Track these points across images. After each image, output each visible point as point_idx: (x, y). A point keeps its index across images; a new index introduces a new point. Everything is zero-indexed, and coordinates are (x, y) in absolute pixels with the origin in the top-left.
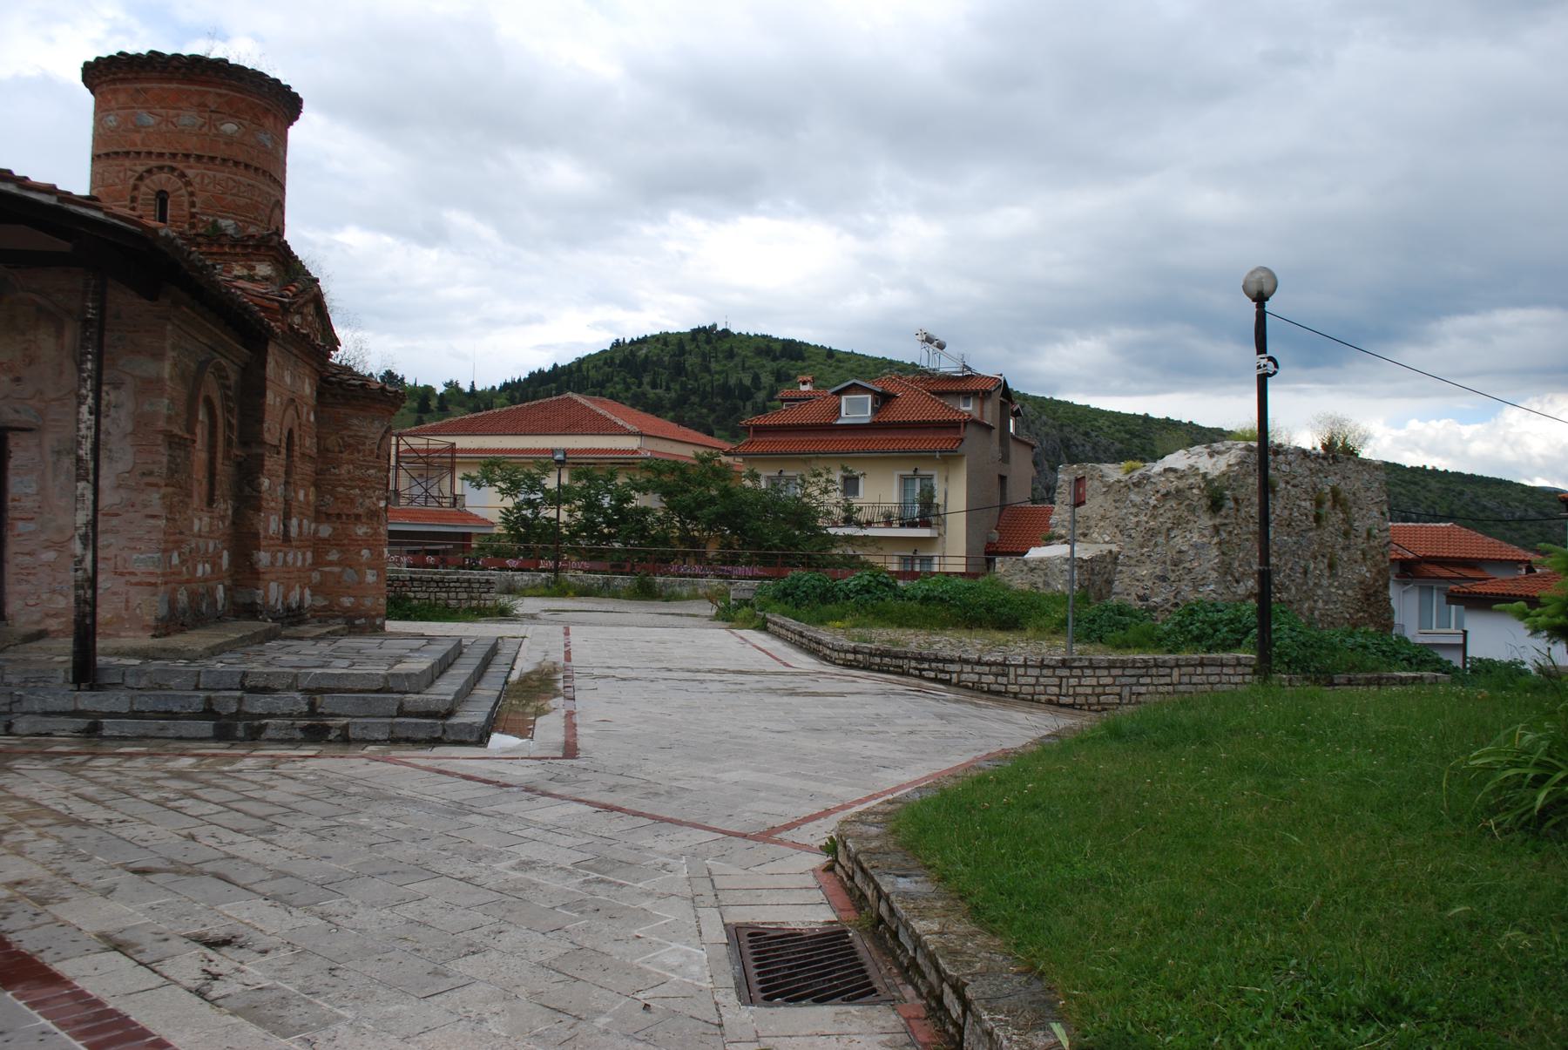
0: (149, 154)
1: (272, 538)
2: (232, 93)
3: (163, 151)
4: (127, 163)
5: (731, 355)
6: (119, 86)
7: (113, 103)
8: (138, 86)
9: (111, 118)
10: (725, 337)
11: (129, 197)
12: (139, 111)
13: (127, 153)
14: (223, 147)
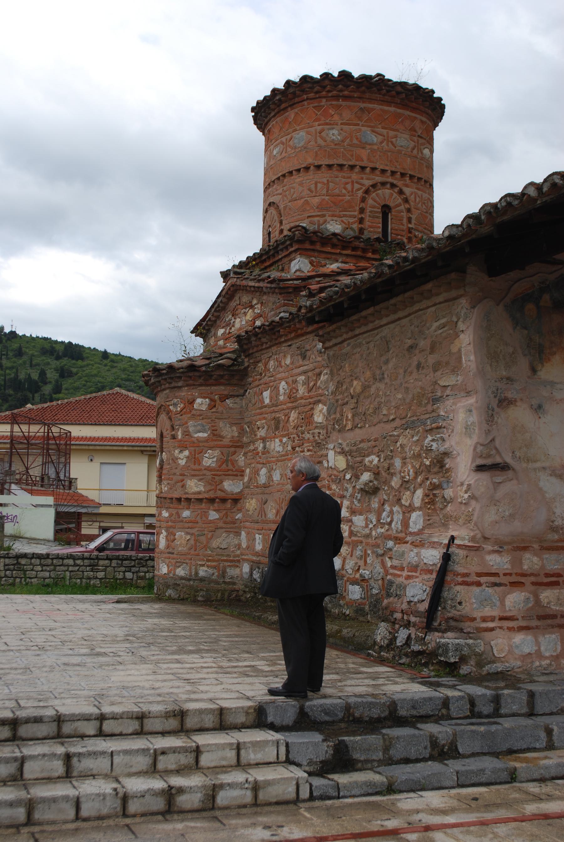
0: (373, 169)
2: (428, 122)
3: (387, 168)
4: (354, 176)
5: (19, 353)
6: (341, 102)
7: (336, 117)
8: (362, 105)
9: (335, 132)
10: (13, 338)
11: (358, 208)
12: (363, 129)
13: (352, 167)
14: (425, 169)
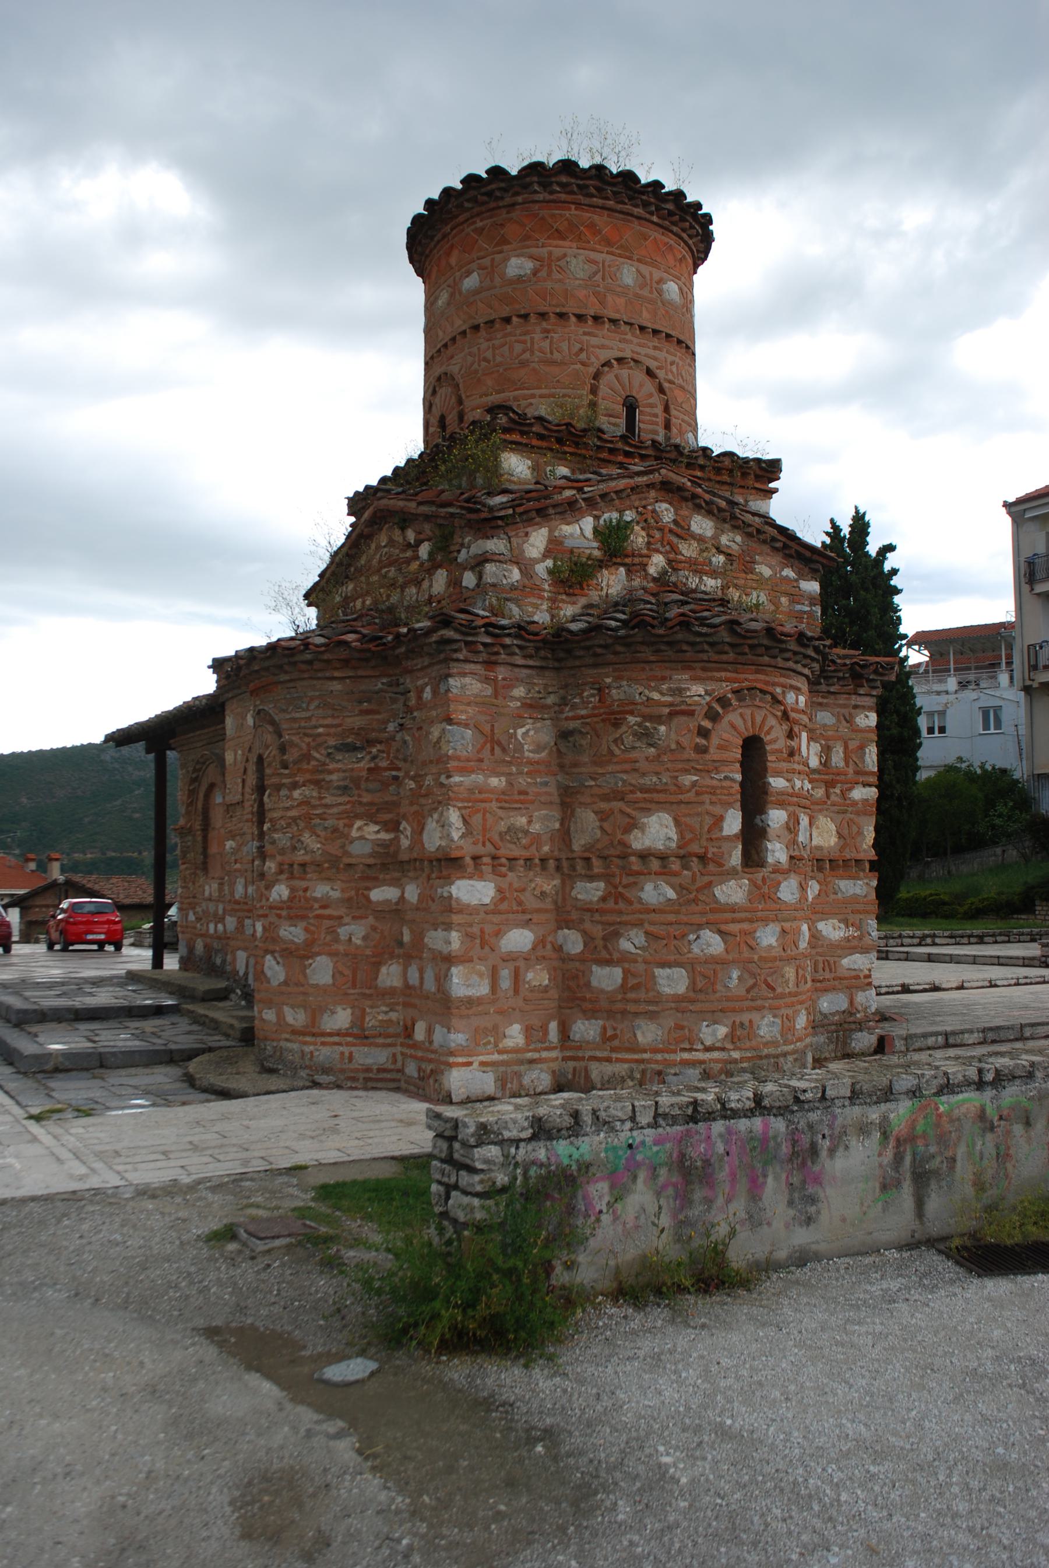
1: (237, 902)
